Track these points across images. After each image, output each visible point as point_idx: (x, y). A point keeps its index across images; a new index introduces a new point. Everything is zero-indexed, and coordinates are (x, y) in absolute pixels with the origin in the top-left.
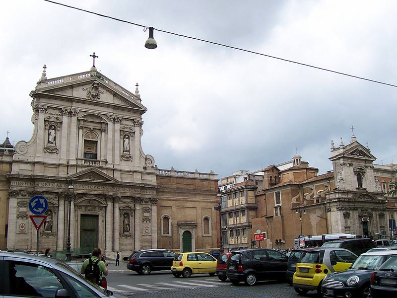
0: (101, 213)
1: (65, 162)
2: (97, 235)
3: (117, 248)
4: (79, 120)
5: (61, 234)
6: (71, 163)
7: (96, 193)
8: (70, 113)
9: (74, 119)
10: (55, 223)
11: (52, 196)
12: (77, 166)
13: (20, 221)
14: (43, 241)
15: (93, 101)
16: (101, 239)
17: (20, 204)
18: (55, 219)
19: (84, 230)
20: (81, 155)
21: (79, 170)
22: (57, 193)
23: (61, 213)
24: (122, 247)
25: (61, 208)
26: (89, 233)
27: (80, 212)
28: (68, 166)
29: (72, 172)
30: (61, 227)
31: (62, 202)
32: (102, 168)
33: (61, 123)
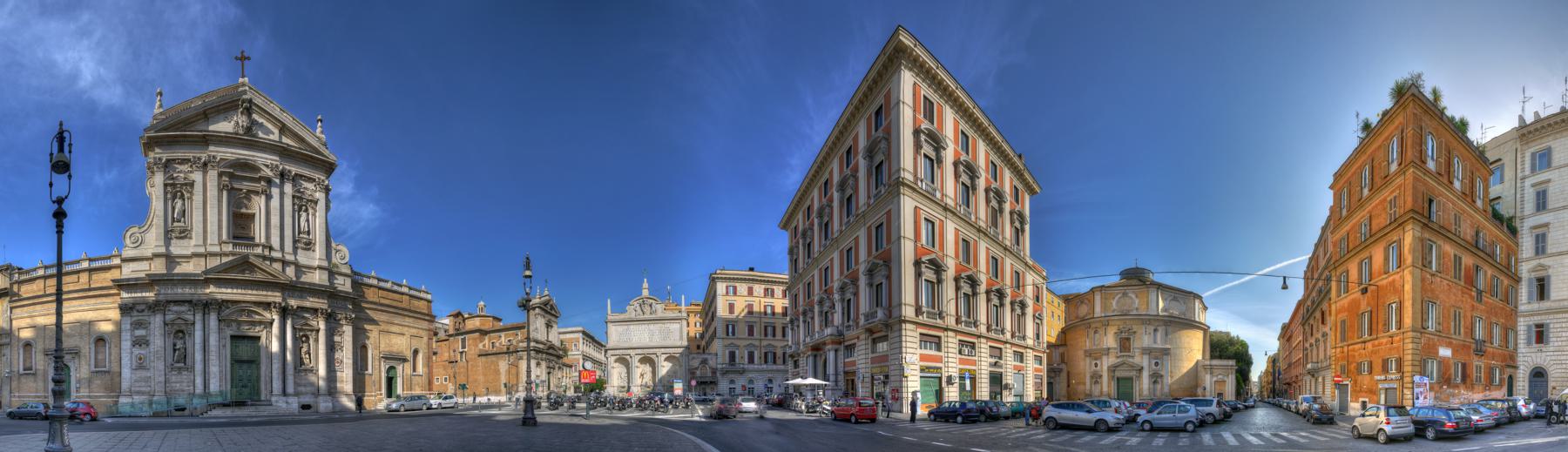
0: (263, 335)
1: (202, 250)
2: (258, 369)
3: (290, 389)
4: (220, 175)
5: (199, 367)
6: (210, 249)
7: (253, 299)
8: (205, 164)
9: (213, 174)
10: (189, 350)
11: (184, 308)
12: (221, 255)
13: (137, 351)
14: (174, 379)
15: (247, 139)
16: (317, 340)
17: (138, 325)
18: (189, 345)
19: (237, 361)
20: (224, 237)
21: (225, 260)
22: (190, 302)
23: (198, 334)
24: (302, 389)
25: (198, 326)
26: (245, 366)
27: (229, 332)
28: (205, 256)
29: (214, 262)
30: (198, 357)
31: (199, 317)
32: (265, 258)
33: (192, 184)
